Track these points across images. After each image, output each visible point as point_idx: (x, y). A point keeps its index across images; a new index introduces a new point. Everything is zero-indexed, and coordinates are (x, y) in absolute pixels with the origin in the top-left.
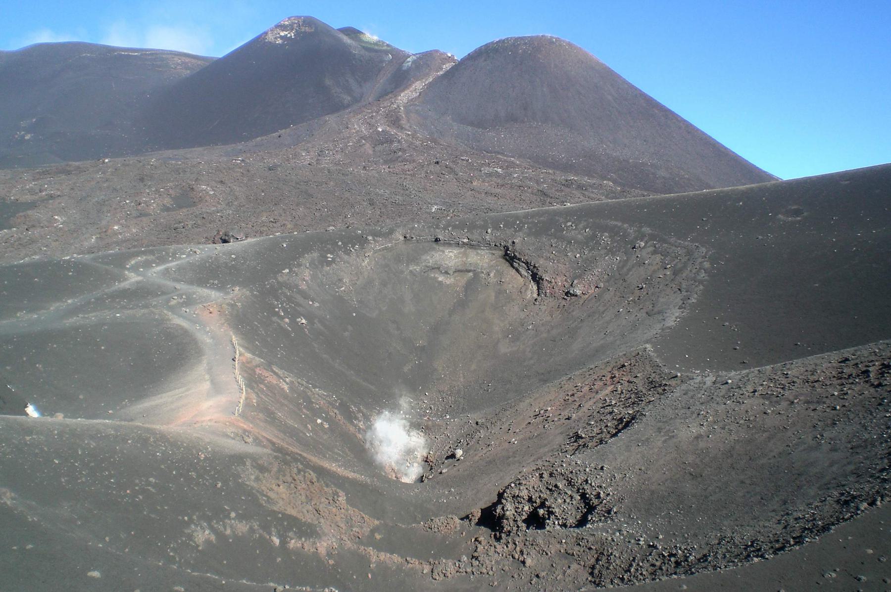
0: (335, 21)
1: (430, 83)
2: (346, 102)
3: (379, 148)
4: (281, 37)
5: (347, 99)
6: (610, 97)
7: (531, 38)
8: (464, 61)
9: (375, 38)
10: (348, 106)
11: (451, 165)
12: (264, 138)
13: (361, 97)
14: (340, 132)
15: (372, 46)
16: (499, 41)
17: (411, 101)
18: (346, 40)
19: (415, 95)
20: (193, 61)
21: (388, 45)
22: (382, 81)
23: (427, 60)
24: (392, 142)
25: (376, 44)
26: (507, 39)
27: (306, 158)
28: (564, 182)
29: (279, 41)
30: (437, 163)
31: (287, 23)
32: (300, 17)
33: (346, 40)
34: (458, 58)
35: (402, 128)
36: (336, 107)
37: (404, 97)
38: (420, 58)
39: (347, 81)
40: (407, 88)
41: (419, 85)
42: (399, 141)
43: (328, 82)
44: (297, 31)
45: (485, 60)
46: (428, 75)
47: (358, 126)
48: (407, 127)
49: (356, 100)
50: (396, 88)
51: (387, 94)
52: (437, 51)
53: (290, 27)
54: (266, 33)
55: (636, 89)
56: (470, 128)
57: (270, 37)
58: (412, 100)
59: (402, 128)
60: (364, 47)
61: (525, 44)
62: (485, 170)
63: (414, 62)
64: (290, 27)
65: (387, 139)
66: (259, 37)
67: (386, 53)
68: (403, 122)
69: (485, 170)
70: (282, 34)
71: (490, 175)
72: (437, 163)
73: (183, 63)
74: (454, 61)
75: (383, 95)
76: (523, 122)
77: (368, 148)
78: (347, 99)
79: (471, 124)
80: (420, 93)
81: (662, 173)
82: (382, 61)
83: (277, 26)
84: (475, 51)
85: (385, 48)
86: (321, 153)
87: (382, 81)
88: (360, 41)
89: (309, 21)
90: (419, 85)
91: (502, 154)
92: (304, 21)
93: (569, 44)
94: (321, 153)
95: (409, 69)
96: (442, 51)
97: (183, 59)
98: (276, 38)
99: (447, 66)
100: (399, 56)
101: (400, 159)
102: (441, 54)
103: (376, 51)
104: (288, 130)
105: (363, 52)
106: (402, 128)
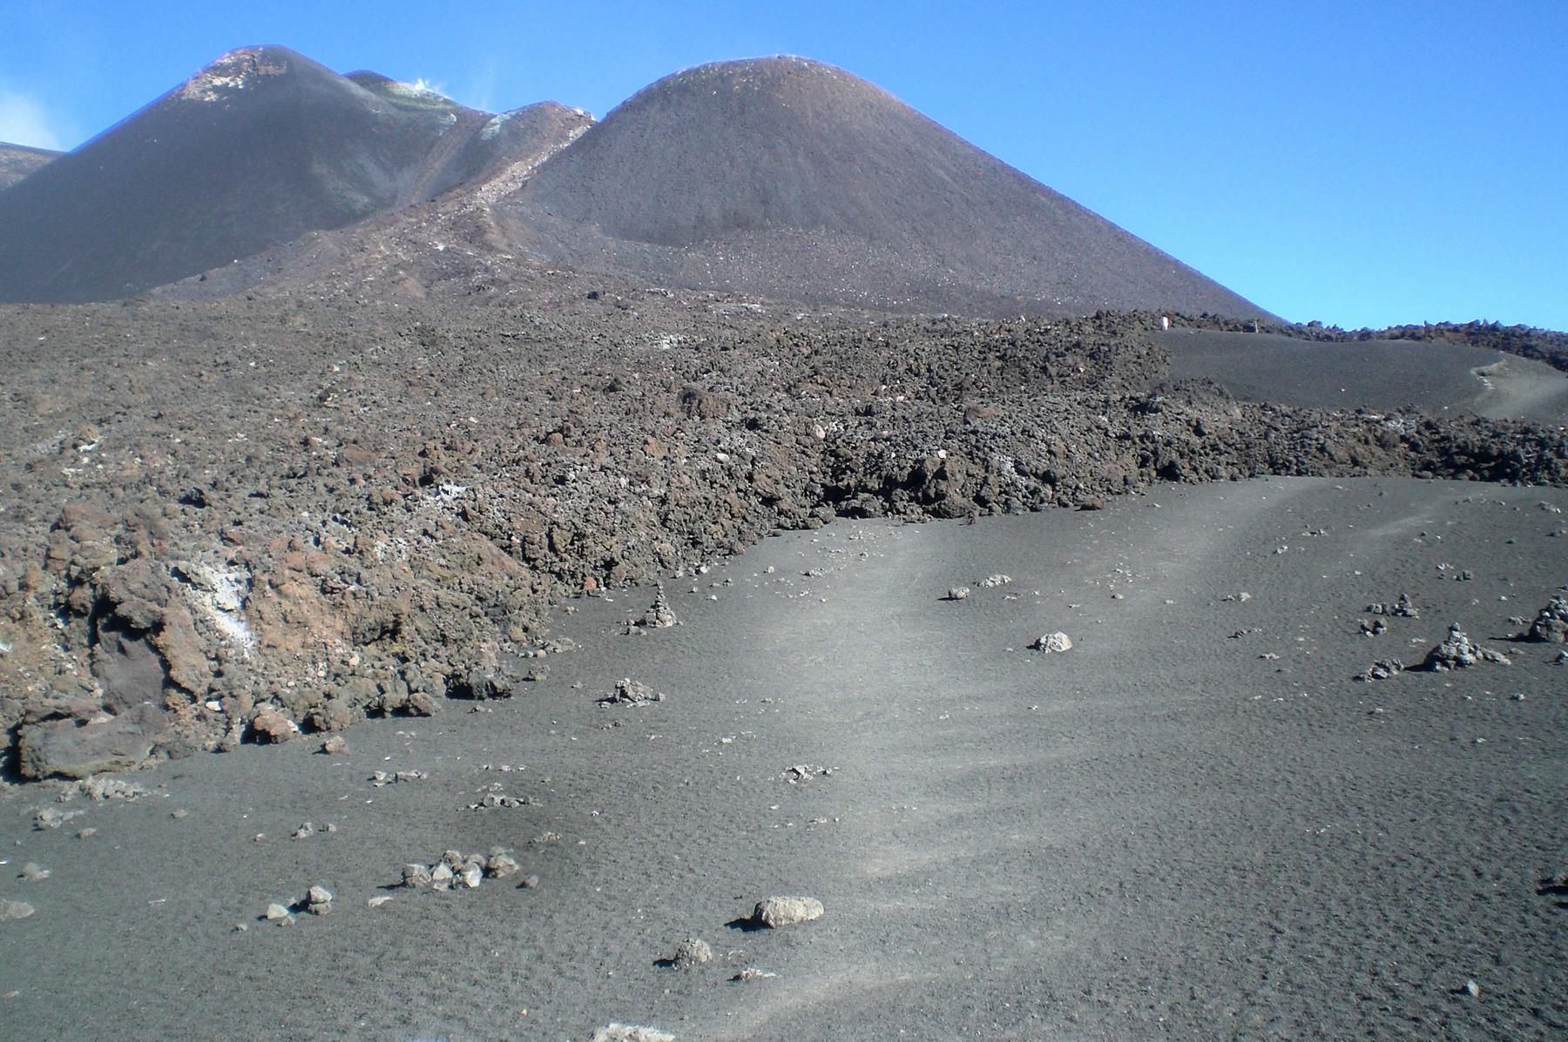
1: (544, 164)
2: (359, 206)
4: (216, 89)
5: (362, 200)
6: (941, 173)
7: (757, 62)
8: (611, 117)
9: (419, 87)
10: (365, 215)
13: (394, 197)
14: (344, 259)
15: (414, 104)
16: (689, 72)
19: (512, 187)
20: (34, 157)
21: (446, 102)
22: (437, 164)
23: (529, 124)
24: (469, 273)
25: (417, 100)
26: (705, 67)
29: (212, 97)
30: (594, 296)
32: (256, 48)
35: (491, 249)
37: (488, 193)
38: (517, 117)
39: (362, 166)
40: (496, 172)
41: (520, 169)
42: (487, 270)
43: (318, 169)
45: (663, 109)
46: (536, 149)
48: (502, 246)
49: (381, 203)
50: (470, 174)
52: (554, 105)
53: (237, 69)
54: (184, 86)
55: (991, 158)
57: (193, 91)
60: (395, 105)
61: (745, 74)
63: (505, 124)
64: (237, 69)
66: (172, 92)
67: (445, 113)
68: (493, 236)
70: (218, 82)
72: (594, 296)
73: (11, 161)
74: (590, 122)
76: (764, 228)
78: (362, 200)
79: (648, 237)
80: (525, 184)
82: (435, 127)
83: (206, 70)
84: (638, 95)
85: (440, 106)
87: (437, 164)
88: (388, 94)
89: (274, 56)
90: (520, 169)
92: (264, 56)
93: (838, 71)
95: (496, 139)
98: (204, 91)
99: (576, 133)
102: (564, 110)
105: (393, 111)
106: (491, 249)
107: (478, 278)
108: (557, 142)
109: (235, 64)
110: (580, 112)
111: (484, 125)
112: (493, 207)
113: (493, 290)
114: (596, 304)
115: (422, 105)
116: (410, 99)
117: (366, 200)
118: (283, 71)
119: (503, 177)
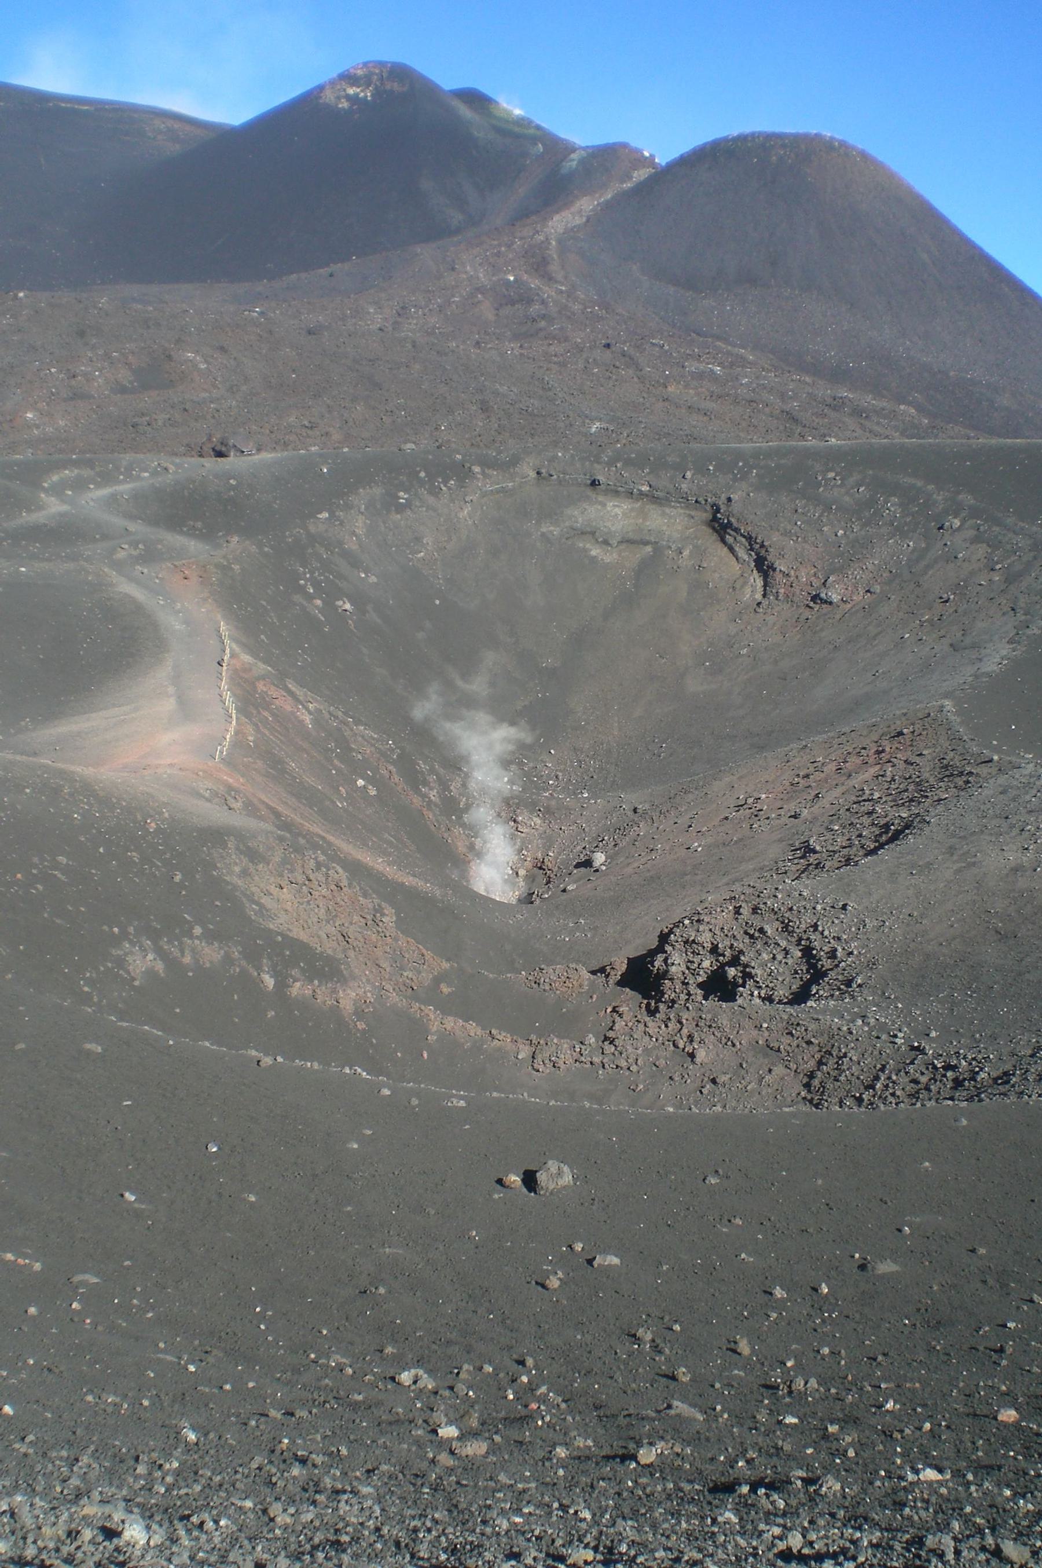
0: (447, 75)
1: (607, 202)
3: (507, 311)
4: (348, 97)
5: (456, 217)
9: (518, 112)
10: (458, 231)
11: (632, 352)
12: (303, 275)
17: (571, 232)
18: (465, 111)
19: (579, 221)
21: (538, 128)
24: (530, 301)
27: (375, 318)
28: (829, 401)
29: (344, 104)
30: (608, 346)
31: (360, 72)
33: (465, 111)
34: (662, 160)
36: (436, 231)
37: (560, 222)
40: (567, 205)
41: (586, 205)
42: (543, 302)
44: (376, 88)
47: (472, 268)
48: (559, 276)
51: (527, 216)
52: (624, 146)
53: (365, 81)
54: (321, 88)
56: (672, 289)
57: (329, 96)
58: (572, 229)
59: (551, 279)
62: (692, 366)
63: (582, 161)
65: (523, 297)
67: (534, 140)
68: (554, 268)
69: (692, 366)
70: (351, 91)
71: (700, 376)
72: (608, 346)
75: (523, 215)
77: (487, 310)
78: (456, 217)
80: (588, 221)
81: (1005, 400)
85: (532, 131)
86: (403, 311)
89: (400, 73)
90: (586, 205)
91: (726, 340)
94: (403, 311)
96: (635, 143)
97: (170, 123)
98: (338, 98)
99: (641, 175)
100: (557, 148)
101: (542, 334)
103: (520, 136)
104: (347, 266)
107: (535, 309)
108: (623, 182)
109: (366, 76)
110: (646, 154)
111: (565, 157)
112: (559, 242)
113: (543, 324)
114: (608, 352)
115: (517, 129)
116: (507, 121)
117: (461, 217)
118: (405, 89)
119: (572, 210)
